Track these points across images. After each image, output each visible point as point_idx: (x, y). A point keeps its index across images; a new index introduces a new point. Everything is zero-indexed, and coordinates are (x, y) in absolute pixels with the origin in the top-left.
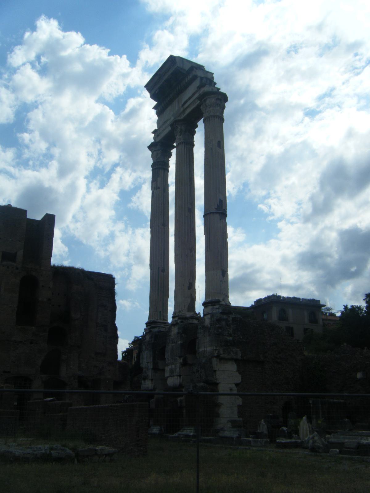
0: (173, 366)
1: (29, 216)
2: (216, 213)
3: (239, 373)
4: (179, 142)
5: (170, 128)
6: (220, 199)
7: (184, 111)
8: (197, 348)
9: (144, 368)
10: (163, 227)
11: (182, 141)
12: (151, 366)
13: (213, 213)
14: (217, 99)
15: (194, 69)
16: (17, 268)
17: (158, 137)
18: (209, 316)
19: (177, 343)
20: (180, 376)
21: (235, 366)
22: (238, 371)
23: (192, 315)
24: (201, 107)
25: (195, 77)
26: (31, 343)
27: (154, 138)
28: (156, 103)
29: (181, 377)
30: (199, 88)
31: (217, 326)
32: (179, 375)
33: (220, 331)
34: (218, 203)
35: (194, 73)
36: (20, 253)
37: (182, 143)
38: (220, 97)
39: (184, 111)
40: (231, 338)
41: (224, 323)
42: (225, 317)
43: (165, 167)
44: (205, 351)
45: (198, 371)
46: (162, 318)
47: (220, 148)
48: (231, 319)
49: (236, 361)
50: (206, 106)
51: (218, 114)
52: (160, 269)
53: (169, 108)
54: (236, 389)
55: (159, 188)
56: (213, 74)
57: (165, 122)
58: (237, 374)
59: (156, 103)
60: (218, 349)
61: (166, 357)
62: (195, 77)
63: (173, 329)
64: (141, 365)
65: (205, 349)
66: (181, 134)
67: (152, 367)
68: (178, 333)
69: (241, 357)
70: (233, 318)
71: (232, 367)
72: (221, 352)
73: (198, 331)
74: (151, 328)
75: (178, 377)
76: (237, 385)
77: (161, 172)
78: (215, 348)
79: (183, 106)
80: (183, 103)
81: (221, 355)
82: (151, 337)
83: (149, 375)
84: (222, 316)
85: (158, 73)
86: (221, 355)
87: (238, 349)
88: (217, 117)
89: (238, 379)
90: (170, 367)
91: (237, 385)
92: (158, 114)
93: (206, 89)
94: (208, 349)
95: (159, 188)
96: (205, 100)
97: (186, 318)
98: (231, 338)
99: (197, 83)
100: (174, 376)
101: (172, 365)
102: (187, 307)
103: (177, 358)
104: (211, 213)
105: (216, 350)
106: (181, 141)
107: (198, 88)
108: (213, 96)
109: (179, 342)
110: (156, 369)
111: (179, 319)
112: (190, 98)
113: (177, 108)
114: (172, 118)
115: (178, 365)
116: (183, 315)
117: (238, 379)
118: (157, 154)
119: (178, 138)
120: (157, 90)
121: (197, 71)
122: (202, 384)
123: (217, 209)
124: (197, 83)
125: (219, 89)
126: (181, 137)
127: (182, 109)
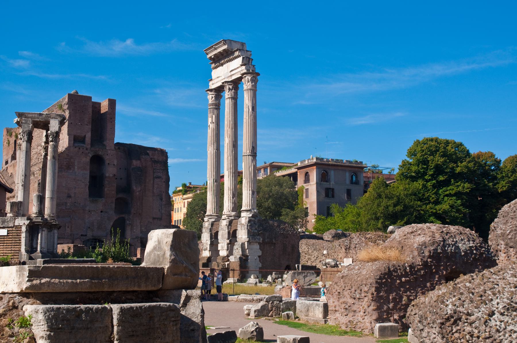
1: (93, 100)
11: (230, 96)
12: (209, 243)
16: (87, 149)
26: (101, 212)
36: (89, 136)
39: (231, 76)
41: (253, 223)
49: (259, 243)
76: (259, 257)
82: (209, 225)
89: (260, 253)
91: (259, 257)
96: (245, 77)
110: (212, 244)
112: (235, 69)
114: (223, 77)
117: (260, 253)
118: (212, 97)
127: (230, 74)
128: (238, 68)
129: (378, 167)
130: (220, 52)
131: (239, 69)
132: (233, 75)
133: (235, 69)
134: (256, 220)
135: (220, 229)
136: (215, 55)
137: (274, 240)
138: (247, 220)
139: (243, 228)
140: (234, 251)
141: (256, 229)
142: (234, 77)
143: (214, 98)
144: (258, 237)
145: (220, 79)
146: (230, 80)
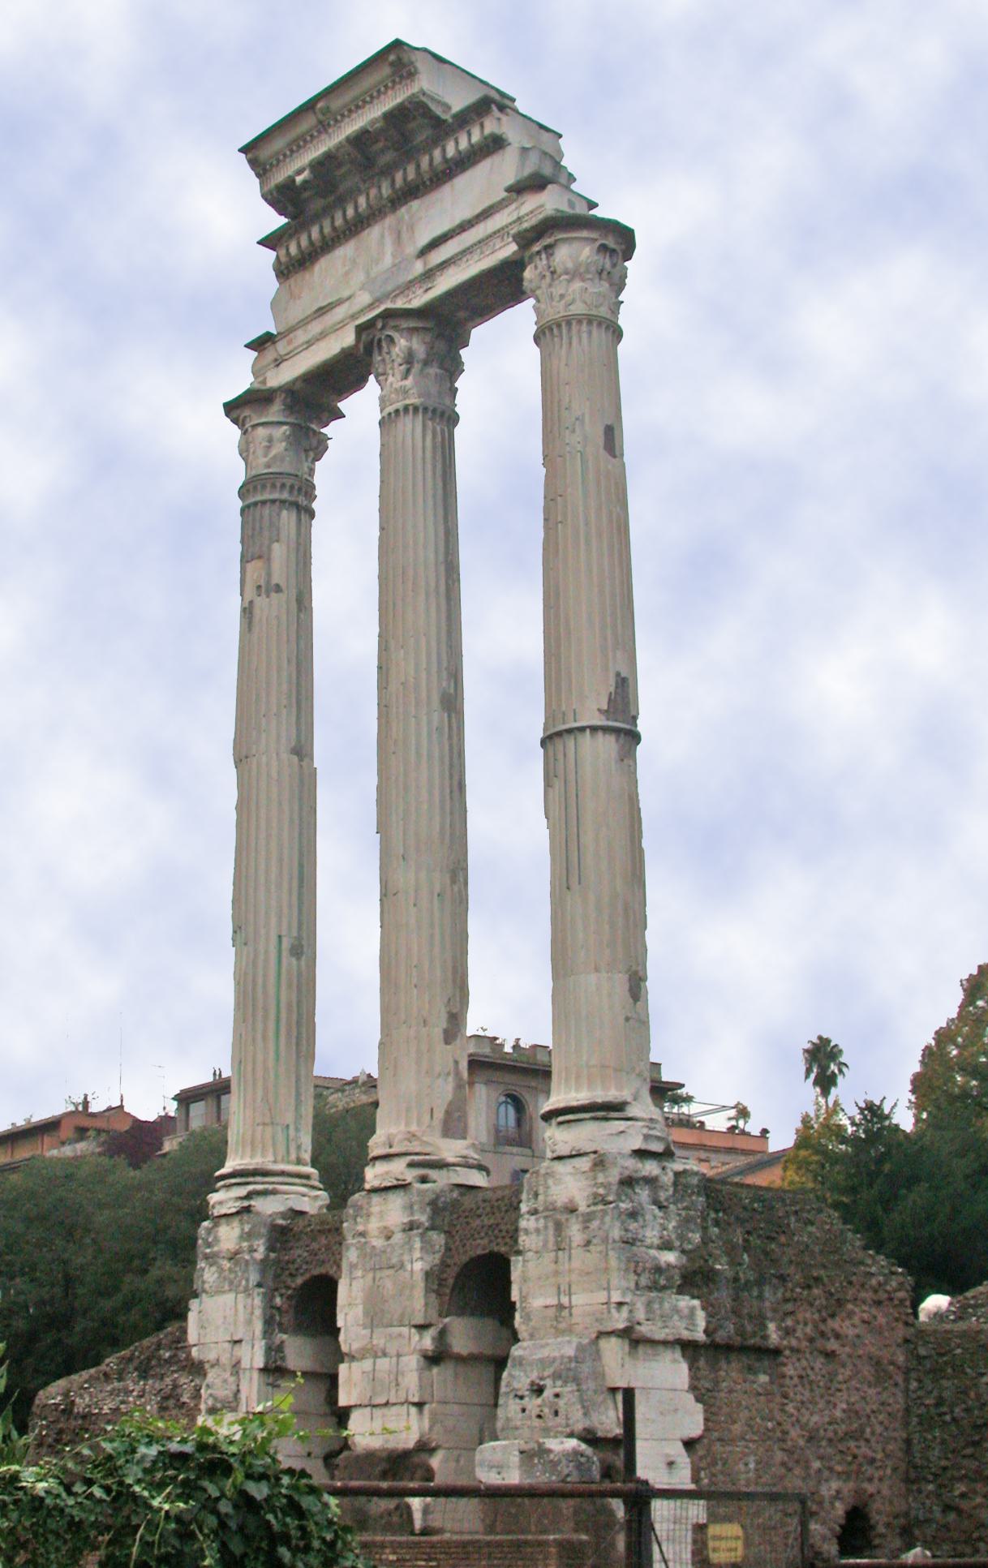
0: (384, 1364)
2: (605, 729)
3: (698, 1400)
4: (399, 405)
5: (347, 338)
6: (618, 674)
7: (429, 275)
8: (515, 1295)
9: (212, 1366)
10: (295, 758)
12: (254, 1356)
13: (594, 729)
14: (603, 248)
15: (494, 107)
18: (584, 1164)
19: (402, 1266)
20: (420, 1405)
21: (684, 1367)
22: (693, 1388)
23: (465, 1152)
24: (528, 274)
25: (496, 144)
27: (257, 371)
28: (283, 220)
29: (427, 1407)
30: (519, 189)
31: (622, 1205)
32: (416, 1400)
33: (633, 1226)
34: (612, 689)
35: (490, 126)
37: (416, 409)
38: (611, 242)
40: (670, 1257)
42: (650, 1168)
43: (299, 498)
44: (561, 1307)
45: (539, 1390)
46: (293, 1156)
47: (615, 456)
48: (671, 1174)
49: (688, 1348)
50: (553, 273)
51: (603, 311)
52: (285, 940)
53: (345, 252)
54: (688, 1460)
55: (278, 589)
56: (560, 136)
57: (321, 308)
58: (690, 1397)
59: (283, 220)
60: (627, 1300)
61: (340, 1323)
63: (375, 1209)
64: (194, 1352)
65: (565, 1300)
66: (408, 371)
67: (260, 1362)
68: (411, 1227)
69: (705, 1331)
70: (677, 1174)
71: (673, 1372)
72: (640, 1315)
73: (523, 1224)
74: (249, 1196)
75: (413, 1410)
76: (689, 1444)
77: (288, 518)
78: (616, 1297)
79: (424, 252)
80: (424, 239)
81: (638, 1327)
82: (247, 1236)
83: (243, 1396)
84: (640, 1165)
86: (638, 1327)
87: (696, 1302)
88: (600, 324)
89: (693, 1422)
90: (367, 1364)
91: (689, 1444)
92: (284, 271)
93: (548, 202)
94: (584, 1301)
95: (278, 589)
96: (549, 249)
97: (441, 1165)
98: (670, 1257)
99: (503, 170)
100: (387, 1404)
101: (376, 1356)
102: (439, 1114)
103: (405, 1330)
104: (582, 729)
105: (620, 1304)
106: (408, 402)
107: (509, 190)
108: (585, 234)
109: (418, 1266)
111: (411, 1165)
112: (463, 227)
113: (388, 261)
114: (365, 298)
115: (412, 1362)
116: (427, 1150)
118: (270, 440)
119: (397, 385)
120: (299, 172)
121: (504, 118)
122: (573, 1443)
123: (604, 713)
124: (503, 170)
126: (409, 382)
127: (419, 267)
129: (688, 1099)
130: (361, 140)
133: (463, 227)
134: (668, 1179)
135: (351, 1255)
136: (318, 166)
137: (772, 1326)
138: (614, 1175)
139: (575, 1232)
140: (509, 1409)
141: (666, 1246)
142: (446, 283)
143: (279, 447)
144: (685, 1302)
145: (340, 313)
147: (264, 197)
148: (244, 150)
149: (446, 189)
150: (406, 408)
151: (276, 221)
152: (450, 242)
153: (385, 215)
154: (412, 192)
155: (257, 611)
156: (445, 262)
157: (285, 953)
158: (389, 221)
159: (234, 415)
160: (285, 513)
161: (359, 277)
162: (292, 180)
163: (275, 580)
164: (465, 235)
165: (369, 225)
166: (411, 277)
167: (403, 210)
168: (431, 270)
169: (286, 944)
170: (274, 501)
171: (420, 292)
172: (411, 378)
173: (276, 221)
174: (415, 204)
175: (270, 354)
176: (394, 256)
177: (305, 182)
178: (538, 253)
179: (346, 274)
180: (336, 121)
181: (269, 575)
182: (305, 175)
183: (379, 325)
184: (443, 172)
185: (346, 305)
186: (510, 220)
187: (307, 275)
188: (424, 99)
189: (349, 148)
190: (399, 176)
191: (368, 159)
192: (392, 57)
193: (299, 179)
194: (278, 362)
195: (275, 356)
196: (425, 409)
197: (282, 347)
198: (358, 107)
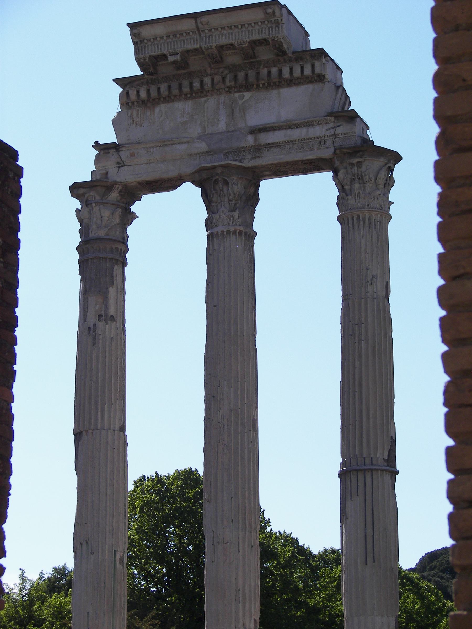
10: (122, 433)
13: (382, 470)
17: (119, 167)
25: (321, 78)
37: (240, 233)
53: (183, 107)
62: (321, 78)
79: (255, 131)
85: (204, 19)
92: (126, 101)
95: (112, 319)
107: (330, 114)
112: (290, 126)
113: (222, 126)
114: (202, 146)
125: (368, 128)
126: (236, 214)
127: (250, 140)
128: (309, 124)
131: (317, 131)
132: (270, 146)
133: (290, 126)
146: (247, 163)
147: (137, 59)
148: (133, 26)
149: (274, 93)
150: (235, 232)
151: (136, 71)
152: (277, 132)
153: (221, 94)
154: (248, 87)
155: (99, 331)
156: (272, 143)
157: (118, 563)
158: (223, 98)
159: (75, 191)
160: (116, 267)
161: (195, 130)
162: (164, 57)
163: (112, 311)
164: (289, 132)
165: (207, 96)
166: (243, 145)
167: (237, 95)
168: (260, 145)
169: (118, 558)
170: (111, 259)
171: (249, 156)
172: (237, 212)
173: (136, 71)
174: (247, 95)
175: (113, 158)
176: (227, 125)
177: (174, 62)
178: (352, 165)
179: (185, 123)
180: (210, 30)
181: (107, 308)
182: (178, 58)
183: (219, 171)
184: (275, 83)
185: (186, 145)
186: (328, 133)
187: (148, 113)
188: (282, 40)
189: (215, 51)
190: (241, 75)
191: (221, 58)
192: (270, 11)
193: (171, 59)
194: (120, 165)
195: (119, 160)
196: (246, 233)
197: (124, 154)
198: (230, 28)
